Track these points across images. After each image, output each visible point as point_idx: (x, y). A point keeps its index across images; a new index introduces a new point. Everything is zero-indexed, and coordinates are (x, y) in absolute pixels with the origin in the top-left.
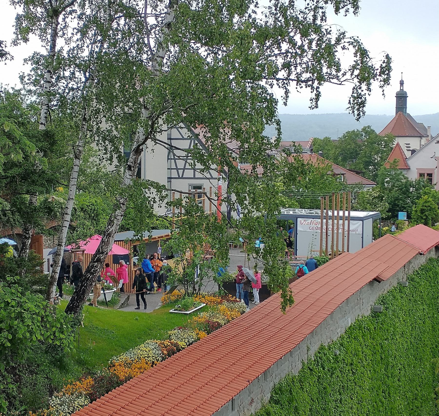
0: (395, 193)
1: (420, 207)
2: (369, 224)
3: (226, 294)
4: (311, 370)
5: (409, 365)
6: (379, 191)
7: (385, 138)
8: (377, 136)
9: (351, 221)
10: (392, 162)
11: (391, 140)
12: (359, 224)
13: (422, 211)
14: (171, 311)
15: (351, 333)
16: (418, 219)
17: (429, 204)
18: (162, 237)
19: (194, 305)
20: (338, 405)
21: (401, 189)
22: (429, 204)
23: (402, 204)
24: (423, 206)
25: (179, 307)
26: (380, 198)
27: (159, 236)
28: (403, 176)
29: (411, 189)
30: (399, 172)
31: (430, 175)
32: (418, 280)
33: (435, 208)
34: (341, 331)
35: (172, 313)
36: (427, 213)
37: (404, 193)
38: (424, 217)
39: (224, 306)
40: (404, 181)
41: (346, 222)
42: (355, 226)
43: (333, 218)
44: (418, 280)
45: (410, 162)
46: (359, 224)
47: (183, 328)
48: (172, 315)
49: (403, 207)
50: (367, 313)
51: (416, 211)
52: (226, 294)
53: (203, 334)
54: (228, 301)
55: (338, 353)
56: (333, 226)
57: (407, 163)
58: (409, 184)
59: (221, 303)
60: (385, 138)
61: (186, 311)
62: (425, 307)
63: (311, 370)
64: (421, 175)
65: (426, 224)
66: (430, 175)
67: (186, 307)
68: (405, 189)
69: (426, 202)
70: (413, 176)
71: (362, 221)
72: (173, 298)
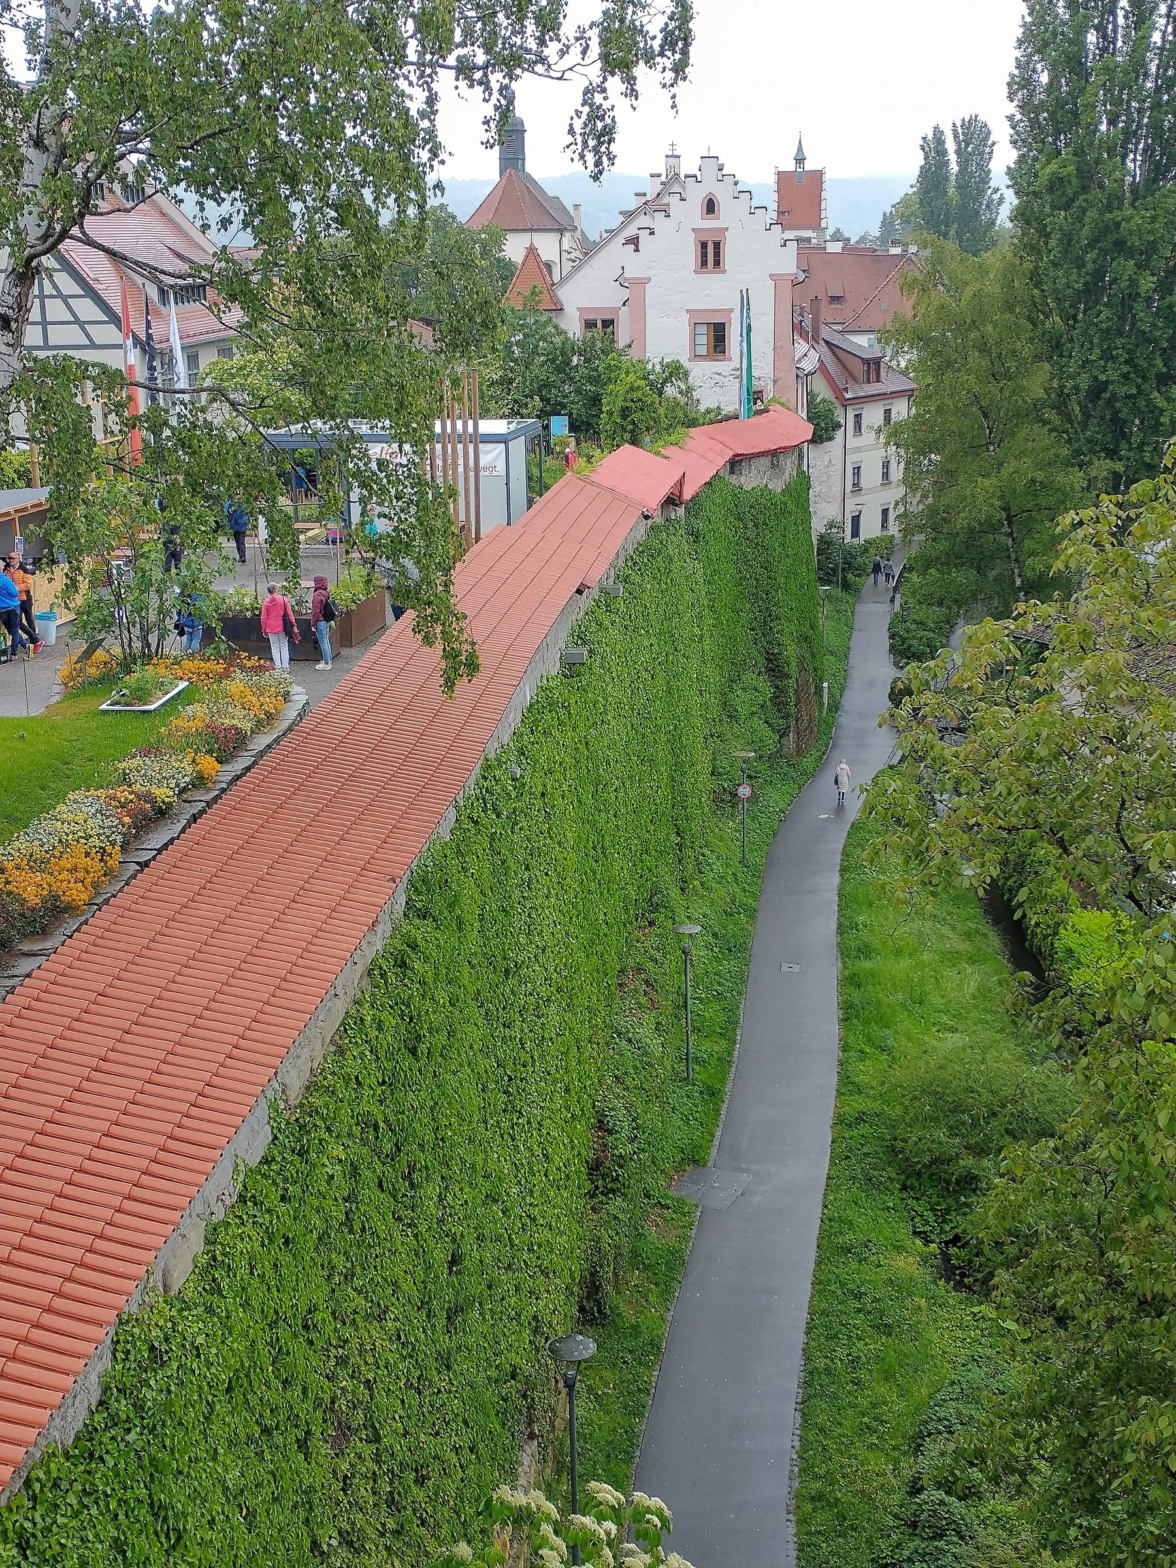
0: (540, 369)
1: (620, 403)
2: (518, 447)
3: (232, 650)
4: (476, 823)
5: (631, 777)
6: (501, 367)
7: (483, 236)
8: (461, 229)
9: (481, 445)
10: (527, 294)
11: (496, 239)
12: (496, 452)
13: (625, 412)
14: (104, 707)
15: (536, 722)
16: (615, 432)
17: (639, 394)
18: (24, 509)
19: (161, 686)
20: (525, 894)
21: (553, 361)
22: (639, 394)
23: (556, 396)
24: (625, 400)
25: (123, 695)
26: (506, 382)
27: (19, 507)
28: (556, 327)
29: (575, 359)
30: (543, 319)
31: (608, 323)
32: (638, 579)
33: (653, 403)
34: (514, 719)
35: (106, 712)
36: (636, 416)
37: (559, 370)
38: (631, 427)
39: (237, 684)
40: (558, 340)
41: (471, 447)
42: (491, 455)
43: (444, 438)
44: (638, 579)
45: (563, 294)
46: (496, 452)
47: (152, 750)
48: (108, 718)
49: (560, 404)
50: (555, 669)
51: (610, 413)
52: (232, 650)
53: (208, 764)
54: (242, 668)
55: (519, 772)
56: (445, 460)
57: (556, 296)
58: (568, 349)
59: (226, 675)
60: (483, 236)
61: (145, 704)
62: (654, 640)
63: (476, 823)
64: (590, 325)
65: (634, 442)
66: (608, 323)
67: (141, 694)
68: (560, 361)
69: (632, 389)
70: (573, 327)
71: (505, 442)
72: (93, 671)
